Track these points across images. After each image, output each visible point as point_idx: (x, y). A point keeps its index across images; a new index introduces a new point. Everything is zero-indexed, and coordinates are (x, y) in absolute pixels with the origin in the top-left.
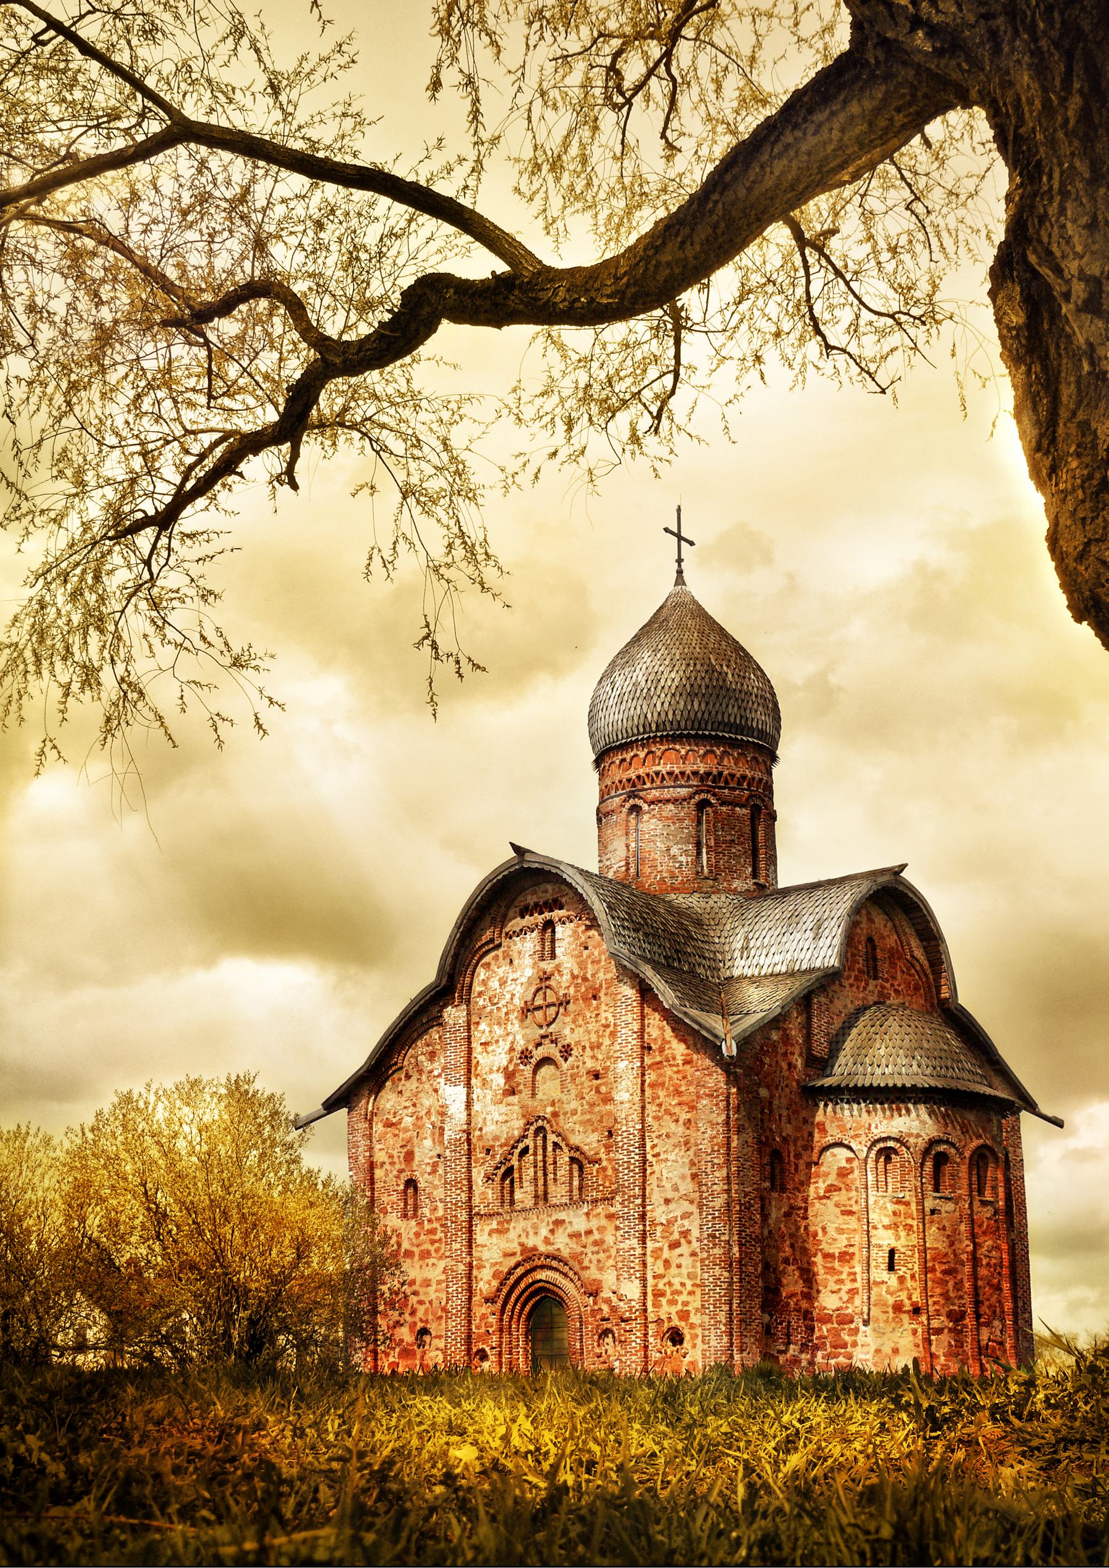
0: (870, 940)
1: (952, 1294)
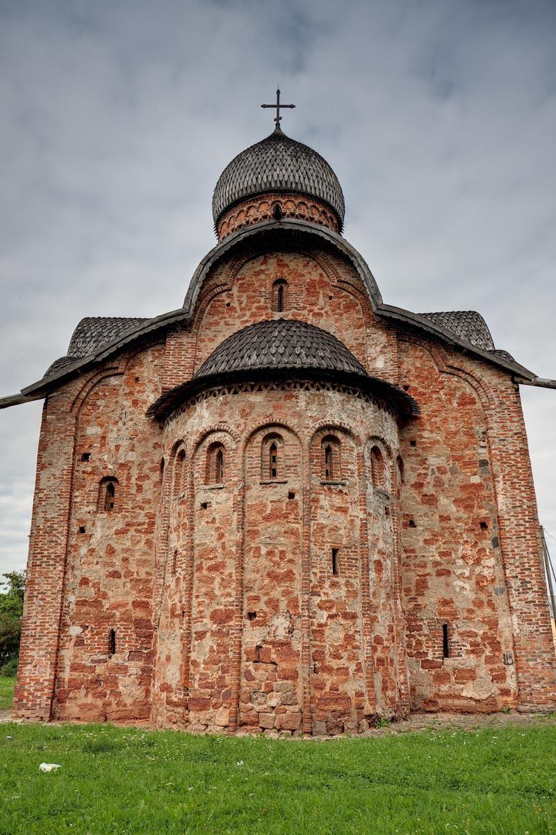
0: (280, 282)
1: (217, 592)
